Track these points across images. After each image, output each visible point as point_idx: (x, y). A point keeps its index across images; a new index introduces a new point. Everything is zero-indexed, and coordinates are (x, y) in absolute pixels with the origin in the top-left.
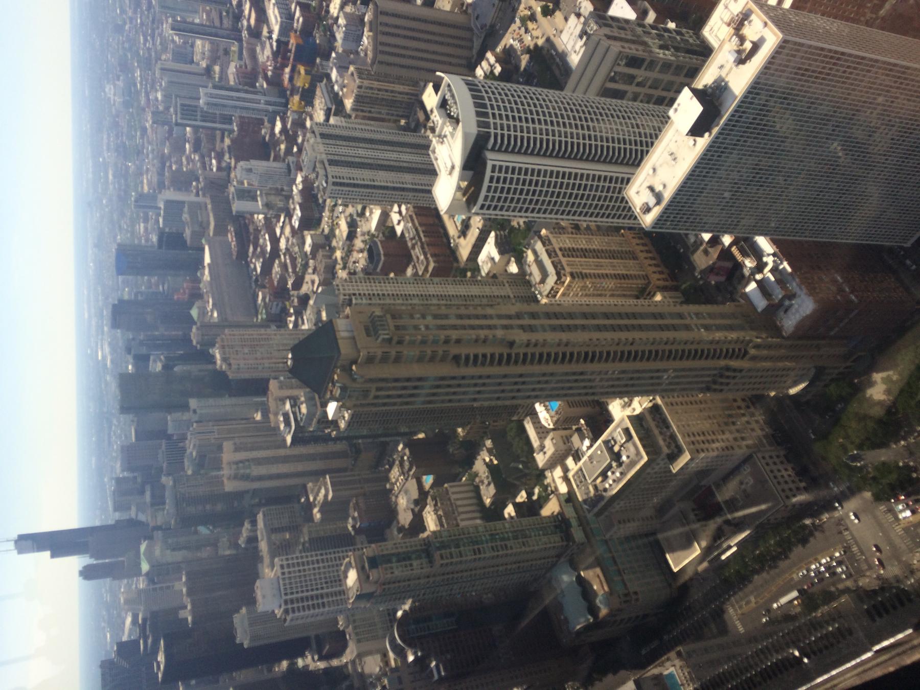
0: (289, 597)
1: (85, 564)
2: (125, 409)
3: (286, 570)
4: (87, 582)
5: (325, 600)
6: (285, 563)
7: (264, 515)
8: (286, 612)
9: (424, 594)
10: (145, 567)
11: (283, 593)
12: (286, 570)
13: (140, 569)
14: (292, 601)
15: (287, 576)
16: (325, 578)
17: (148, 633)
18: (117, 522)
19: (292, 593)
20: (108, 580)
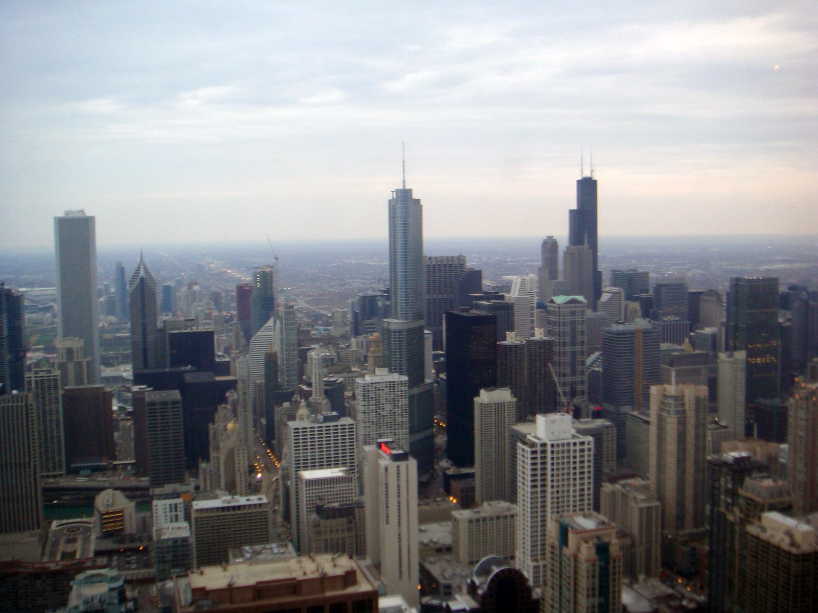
0: (549, 449)
1: (559, 243)
2: (737, 283)
4: (540, 244)
6: (586, 447)
7: (607, 427)
8: (533, 445)
9: (552, 606)
10: (560, 299)
11: (555, 443)
12: (578, 447)
13: (558, 295)
14: (544, 452)
15: (572, 448)
17: (493, 301)
19: (552, 452)
20: (539, 263)
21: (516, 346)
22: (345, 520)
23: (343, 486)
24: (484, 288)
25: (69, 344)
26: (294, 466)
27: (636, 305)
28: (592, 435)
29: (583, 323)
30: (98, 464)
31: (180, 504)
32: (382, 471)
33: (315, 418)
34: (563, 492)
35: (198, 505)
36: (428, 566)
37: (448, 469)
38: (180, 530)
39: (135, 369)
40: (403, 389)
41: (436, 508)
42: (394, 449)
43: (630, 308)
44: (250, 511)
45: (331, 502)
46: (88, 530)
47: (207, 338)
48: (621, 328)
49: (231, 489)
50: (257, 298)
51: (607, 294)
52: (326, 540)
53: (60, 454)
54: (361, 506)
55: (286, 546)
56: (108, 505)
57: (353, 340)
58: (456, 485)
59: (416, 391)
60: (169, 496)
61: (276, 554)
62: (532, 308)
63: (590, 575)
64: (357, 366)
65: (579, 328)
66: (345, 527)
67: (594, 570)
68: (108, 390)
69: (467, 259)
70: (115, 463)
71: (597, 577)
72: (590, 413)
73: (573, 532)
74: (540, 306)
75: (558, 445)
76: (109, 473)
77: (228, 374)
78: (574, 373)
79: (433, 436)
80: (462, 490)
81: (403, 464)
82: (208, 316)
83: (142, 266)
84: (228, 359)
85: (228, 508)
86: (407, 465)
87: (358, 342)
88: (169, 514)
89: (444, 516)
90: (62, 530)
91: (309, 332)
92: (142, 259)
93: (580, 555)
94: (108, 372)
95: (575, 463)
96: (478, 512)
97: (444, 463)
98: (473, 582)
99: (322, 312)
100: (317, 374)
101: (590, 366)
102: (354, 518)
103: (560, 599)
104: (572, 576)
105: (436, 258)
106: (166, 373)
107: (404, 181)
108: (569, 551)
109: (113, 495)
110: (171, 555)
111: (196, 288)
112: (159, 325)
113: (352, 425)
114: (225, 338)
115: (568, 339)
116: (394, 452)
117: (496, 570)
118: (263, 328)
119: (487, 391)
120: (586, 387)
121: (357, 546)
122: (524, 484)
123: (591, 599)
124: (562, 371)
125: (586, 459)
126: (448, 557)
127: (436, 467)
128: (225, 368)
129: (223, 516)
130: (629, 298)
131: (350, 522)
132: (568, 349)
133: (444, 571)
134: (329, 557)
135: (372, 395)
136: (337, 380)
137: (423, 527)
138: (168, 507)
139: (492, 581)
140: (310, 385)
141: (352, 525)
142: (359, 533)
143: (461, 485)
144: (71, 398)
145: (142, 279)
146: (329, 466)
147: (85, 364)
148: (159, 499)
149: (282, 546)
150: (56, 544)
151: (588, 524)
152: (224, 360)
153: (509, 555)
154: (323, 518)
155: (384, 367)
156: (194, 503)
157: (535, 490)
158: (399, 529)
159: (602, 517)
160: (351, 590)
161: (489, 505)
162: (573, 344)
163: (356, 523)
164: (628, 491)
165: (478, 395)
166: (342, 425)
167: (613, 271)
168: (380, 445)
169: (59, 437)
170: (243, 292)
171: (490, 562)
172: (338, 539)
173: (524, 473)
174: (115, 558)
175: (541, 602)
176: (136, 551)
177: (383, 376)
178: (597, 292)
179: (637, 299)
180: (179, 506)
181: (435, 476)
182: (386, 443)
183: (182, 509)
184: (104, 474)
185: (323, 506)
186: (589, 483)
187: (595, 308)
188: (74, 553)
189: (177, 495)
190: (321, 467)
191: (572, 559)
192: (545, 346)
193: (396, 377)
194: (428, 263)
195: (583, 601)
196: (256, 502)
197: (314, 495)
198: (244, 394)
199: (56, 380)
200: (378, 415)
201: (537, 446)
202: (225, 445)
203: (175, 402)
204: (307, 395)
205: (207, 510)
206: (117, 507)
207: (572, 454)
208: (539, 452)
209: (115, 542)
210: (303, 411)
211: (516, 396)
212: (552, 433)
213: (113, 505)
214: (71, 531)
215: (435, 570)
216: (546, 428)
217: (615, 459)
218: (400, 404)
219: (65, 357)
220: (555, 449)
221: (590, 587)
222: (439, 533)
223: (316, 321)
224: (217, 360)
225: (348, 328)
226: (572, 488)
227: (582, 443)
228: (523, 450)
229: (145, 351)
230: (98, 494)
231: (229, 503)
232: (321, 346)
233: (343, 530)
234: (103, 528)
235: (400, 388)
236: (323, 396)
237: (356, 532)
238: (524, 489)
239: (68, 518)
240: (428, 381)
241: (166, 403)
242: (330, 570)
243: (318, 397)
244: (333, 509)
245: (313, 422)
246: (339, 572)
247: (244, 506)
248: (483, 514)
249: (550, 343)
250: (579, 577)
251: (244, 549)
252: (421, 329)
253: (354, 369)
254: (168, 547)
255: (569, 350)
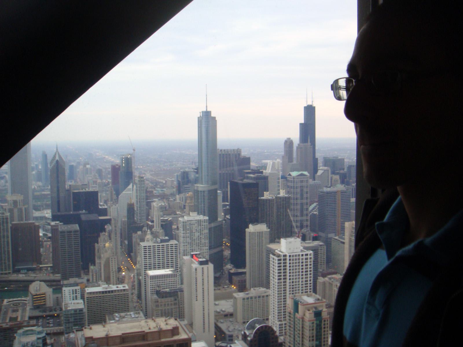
0: (288, 258)
1: (293, 142)
3: (304, 257)
5: (282, 281)
6: (309, 257)
7: (321, 246)
8: (279, 256)
10: (294, 174)
11: (291, 254)
12: (304, 257)
14: (285, 260)
15: (301, 257)
16: (296, 282)
17: (256, 175)
18: (317, 159)
19: (290, 260)
20: (283, 153)
21: (269, 200)
22: (172, 299)
23: (172, 279)
24: (252, 167)
25: (15, 198)
26: (144, 268)
27: (337, 177)
28: (312, 250)
29: (307, 187)
30: (31, 266)
31: (78, 289)
32: (194, 270)
33: (156, 241)
34: (296, 282)
35: (89, 290)
36: (220, 325)
37: (231, 269)
38: (79, 304)
39: (52, 212)
40: (206, 224)
41: (224, 291)
42: (200, 258)
43: (334, 179)
44: (118, 294)
45: (165, 288)
46: (26, 304)
47: (94, 195)
48: (329, 189)
49: (108, 281)
50: (123, 172)
51: (321, 171)
52: (162, 310)
53: (9, 261)
54: (182, 291)
55: (139, 313)
56: (37, 290)
57: (177, 196)
58: (235, 279)
59: (213, 225)
60: (73, 285)
61: (133, 318)
62: (279, 179)
63: (311, 328)
64: (179, 211)
65: (305, 190)
66: (173, 303)
67: (313, 326)
68: (37, 224)
69: (242, 150)
70: (41, 266)
71: (315, 329)
72: (311, 238)
73: (301, 305)
74: (283, 177)
75: (293, 256)
76: (37, 272)
77: (106, 215)
78: (302, 215)
79: (222, 251)
80: (239, 281)
81: (205, 267)
82: (95, 182)
83: (57, 152)
84: (106, 207)
85: (106, 292)
86: (208, 267)
87: (180, 197)
88: (72, 295)
89: (229, 296)
90: (9, 305)
91: (152, 191)
92: (57, 149)
93: (305, 317)
94: (37, 214)
95: (302, 266)
96: (247, 294)
97: (229, 266)
98: (245, 333)
99: (160, 180)
100: (157, 216)
101: (311, 211)
102: (178, 298)
103: (294, 342)
104: (301, 329)
105: (224, 150)
106: (72, 215)
107: (207, 107)
108: (299, 315)
109: (40, 284)
110: (73, 318)
111: (88, 166)
112: (67, 187)
113: (177, 244)
114: (104, 195)
115: (299, 196)
116: (200, 260)
117: (258, 326)
118: (126, 189)
119: (253, 225)
120: (309, 223)
121: (179, 313)
122: (274, 278)
123: (311, 342)
124: (296, 214)
125: (309, 263)
126: (231, 319)
127: (224, 268)
128: (104, 212)
129: (103, 296)
130: (333, 173)
131: (176, 300)
132: (299, 201)
133: (229, 327)
134: (163, 319)
135: (188, 227)
136: (168, 219)
137: (217, 303)
138: (71, 291)
139: (256, 333)
140: (153, 222)
141: (177, 302)
142: (181, 306)
143: (239, 279)
144: (15, 229)
145: (57, 161)
146: (164, 268)
147: (24, 209)
148: (66, 287)
149: (136, 313)
150: (6, 313)
151: (310, 300)
152: (104, 207)
153: (265, 318)
154: (160, 297)
155: (195, 211)
156: (86, 289)
157: (280, 281)
158: (203, 303)
159: (318, 296)
160: (176, 338)
161: (254, 290)
162: (302, 198)
163: (179, 300)
164: (332, 281)
165: (248, 227)
166: (171, 245)
167: (324, 158)
168: (192, 256)
169: (8, 252)
170: (115, 169)
171: (254, 322)
172: (168, 309)
173: (274, 271)
174: (41, 320)
175: (284, 344)
176: (52, 316)
177: (194, 216)
178: (316, 170)
179: (338, 174)
180: (78, 290)
181: (224, 273)
182: (196, 255)
183: (80, 292)
184: (34, 272)
185: (160, 291)
186: (311, 277)
187: (314, 179)
188: (17, 318)
189: (77, 285)
190: (159, 268)
191: (301, 320)
192: (286, 200)
193: (201, 217)
194: (220, 153)
195: (307, 343)
196: (122, 288)
197: (155, 284)
198: (115, 227)
199: (7, 219)
200: (191, 238)
201: (281, 257)
202: (105, 256)
203: (76, 231)
204: (151, 228)
205: (94, 293)
206: (42, 292)
207: (301, 261)
208: (282, 260)
209: (40, 311)
210: (149, 236)
211: (269, 228)
212: (290, 249)
213: (39, 290)
214: (15, 305)
215: (223, 327)
216: (287, 246)
217: (325, 263)
218: (204, 233)
219: (12, 205)
220: (291, 258)
221: (311, 335)
222: (226, 306)
223: (156, 185)
224: (100, 207)
225: (174, 190)
226: (301, 280)
227: (307, 255)
228: (274, 259)
229: (58, 202)
230: (31, 284)
231: (106, 289)
232: (159, 200)
233: (171, 304)
234: (34, 303)
235: (203, 223)
236: (160, 228)
237: (179, 305)
238: (274, 281)
239: (13, 298)
240: (219, 219)
241: (70, 232)
242: (164, 327)
243: (157, 228)
244: (166, 292)
245: (154, 243)
246: (169, 327)
247: (115, 291)
248: (251, 295)
249: (289, 198)
250: (305, 330)
251: (115, 315)
252: (216, 190)
253: (178, 213)
254: (71, 314)
255: (299, 185)
